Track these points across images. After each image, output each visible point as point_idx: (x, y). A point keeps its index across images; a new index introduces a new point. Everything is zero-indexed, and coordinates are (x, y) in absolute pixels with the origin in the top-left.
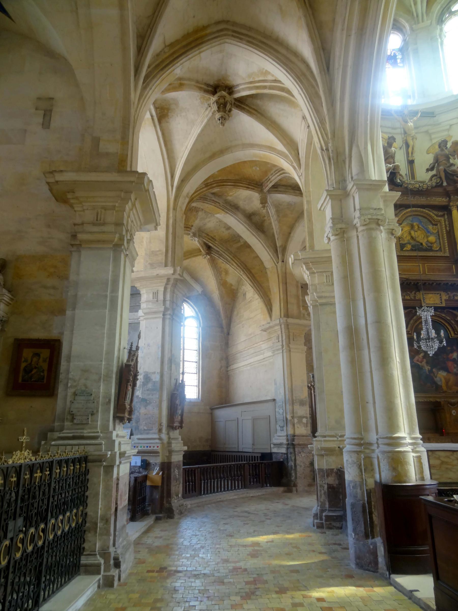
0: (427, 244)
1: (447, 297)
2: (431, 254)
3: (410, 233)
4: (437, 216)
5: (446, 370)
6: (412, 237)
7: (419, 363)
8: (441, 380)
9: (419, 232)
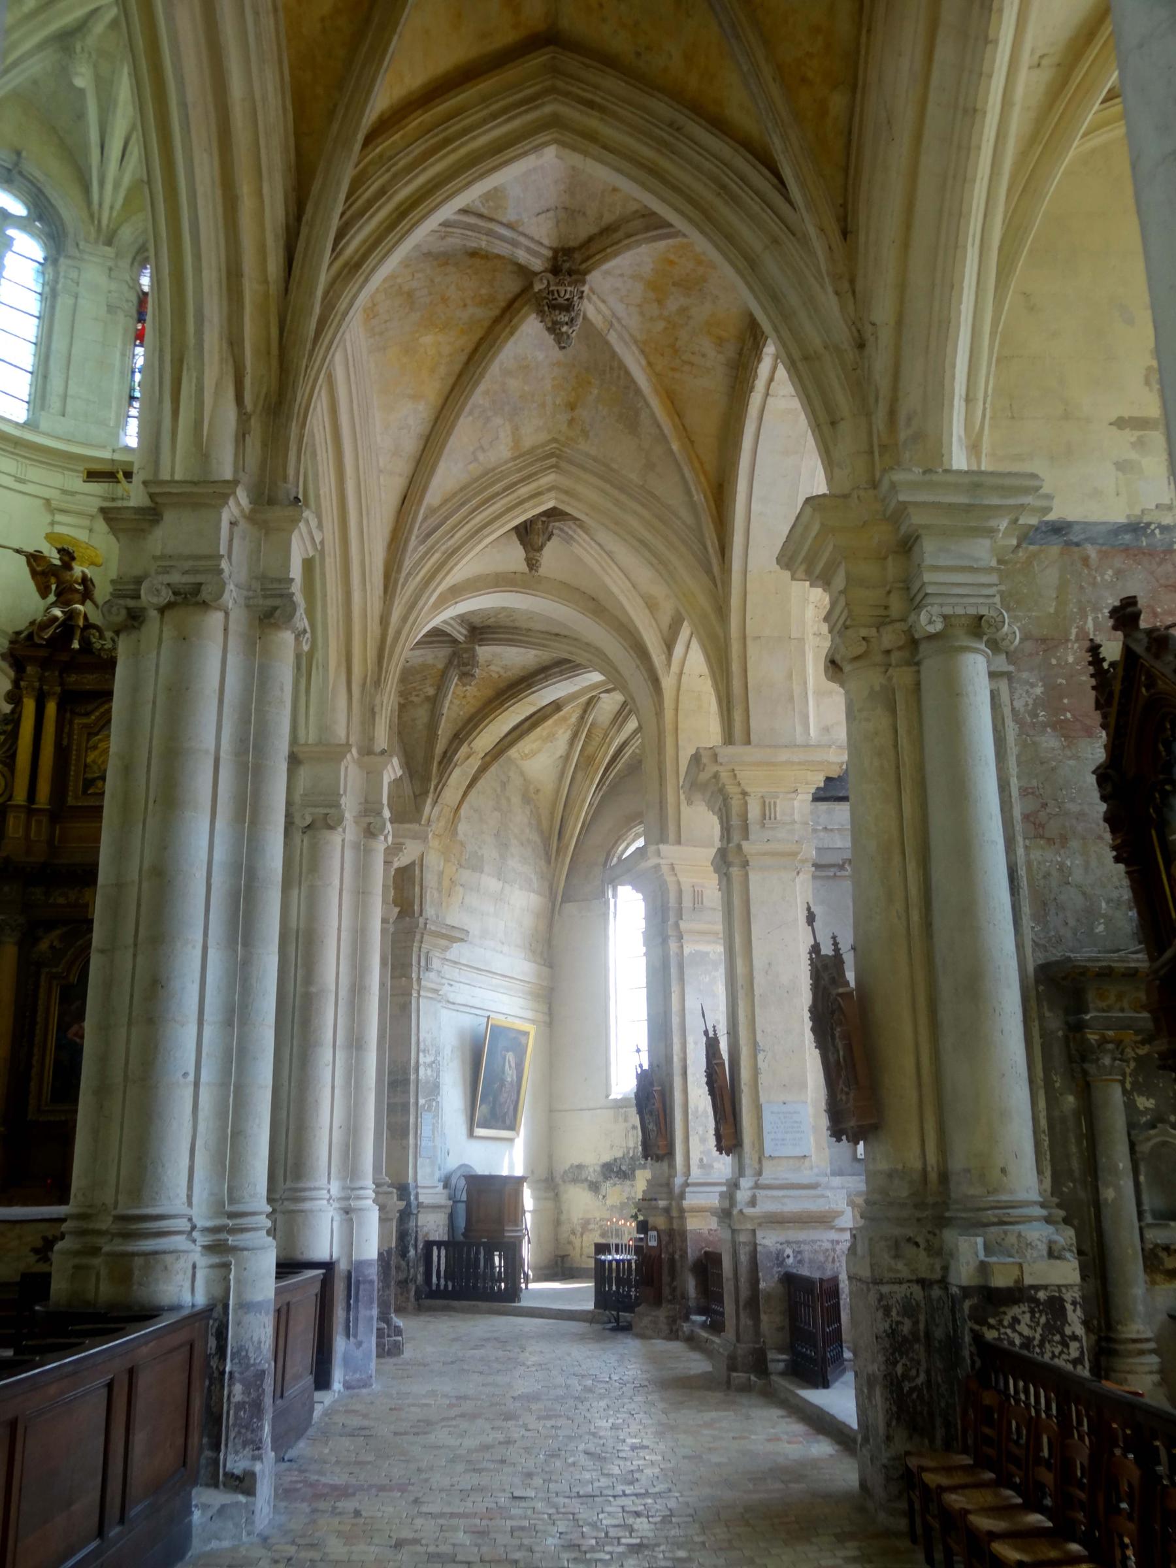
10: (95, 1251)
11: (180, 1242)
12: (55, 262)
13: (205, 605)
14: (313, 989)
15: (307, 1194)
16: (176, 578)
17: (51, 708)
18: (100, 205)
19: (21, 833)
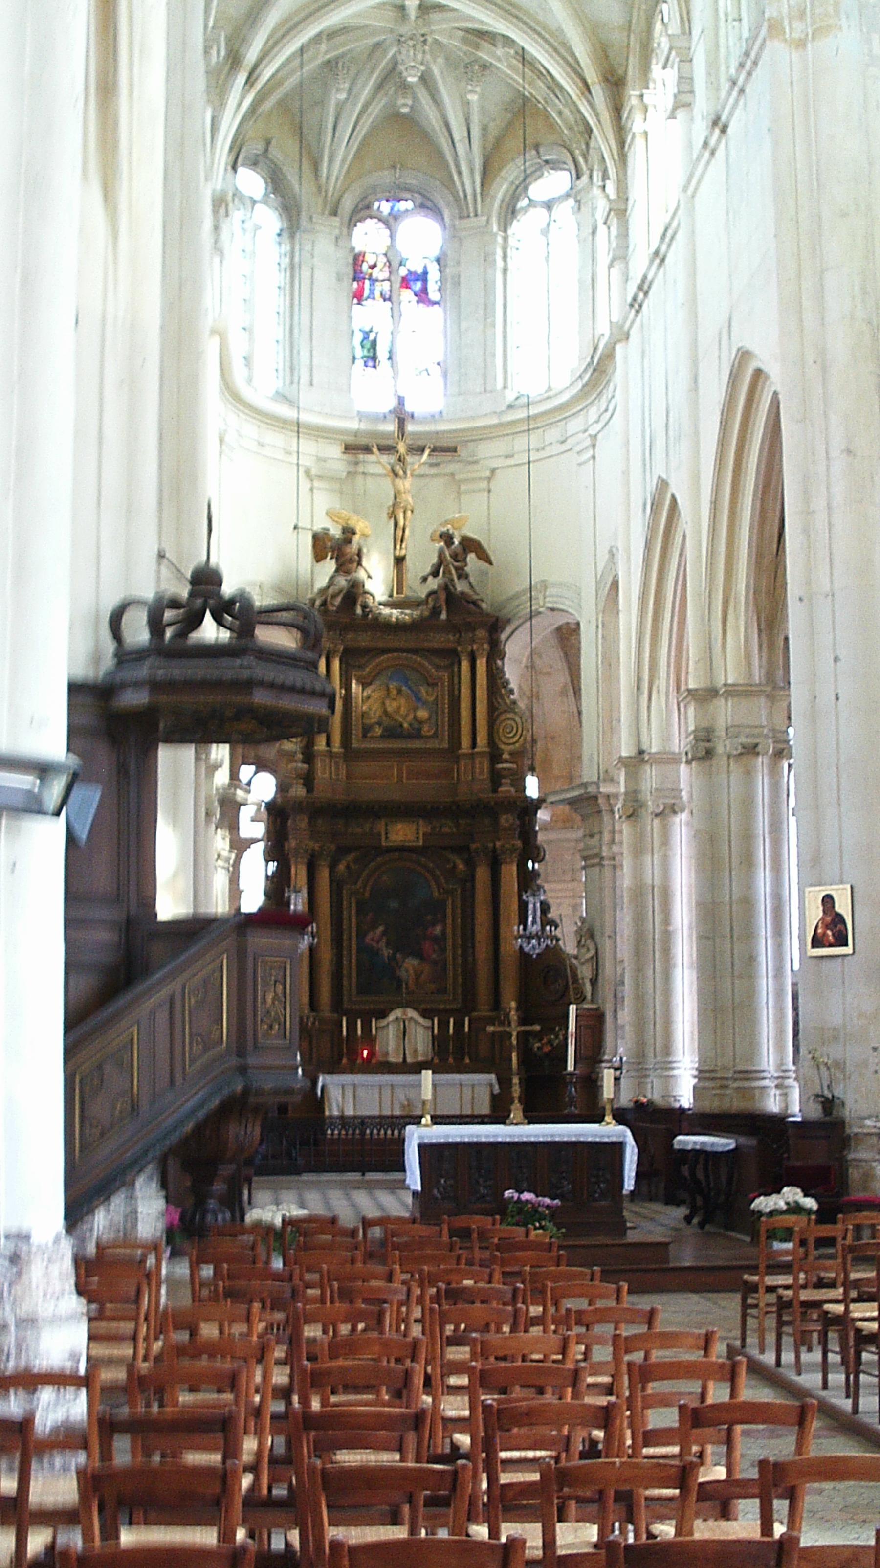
0: (410, 725)
1: (428, 829)
2: (417, 744)
3: (383, 704)
4: (438, 667)
5: (420, 955)
6: (385, 712)
7: (374, 944)
8: (407, 971)
9: (403, 701)
10: (726, 1087)
11: (766, 1083)
12: (292, 236)
13: (758, 754)
14: (671, 928)
15: (675, 1065)
16: (743, 740)
17: (336, 664)
18: (328, 178)
19: (327, 775)
